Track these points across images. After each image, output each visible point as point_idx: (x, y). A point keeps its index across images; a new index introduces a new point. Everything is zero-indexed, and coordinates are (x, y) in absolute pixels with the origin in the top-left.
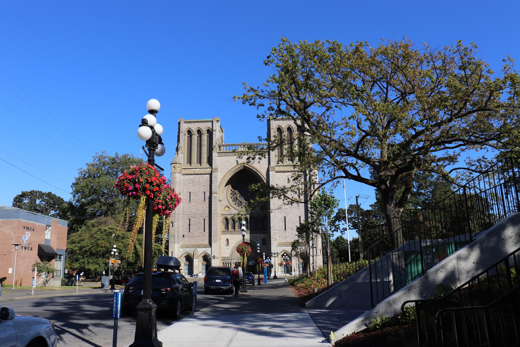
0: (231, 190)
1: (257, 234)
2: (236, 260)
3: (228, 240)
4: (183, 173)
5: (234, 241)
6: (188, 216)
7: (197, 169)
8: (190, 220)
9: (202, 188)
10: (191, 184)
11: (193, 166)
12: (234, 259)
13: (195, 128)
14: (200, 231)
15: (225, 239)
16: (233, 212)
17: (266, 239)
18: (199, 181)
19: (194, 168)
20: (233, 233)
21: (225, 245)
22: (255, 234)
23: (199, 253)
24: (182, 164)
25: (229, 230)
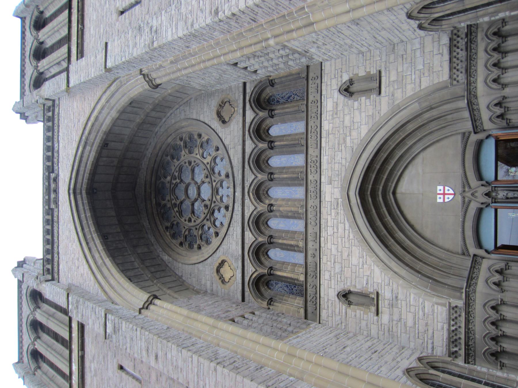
0: (181, 244)
2: (476, 260)
5: (354, 260)
9: (110, 373)
12: (471, 280)
15: (340, 307)
17: (346, 78)
20: (314, 256)
21: (372, 315)
22: (323, 140)
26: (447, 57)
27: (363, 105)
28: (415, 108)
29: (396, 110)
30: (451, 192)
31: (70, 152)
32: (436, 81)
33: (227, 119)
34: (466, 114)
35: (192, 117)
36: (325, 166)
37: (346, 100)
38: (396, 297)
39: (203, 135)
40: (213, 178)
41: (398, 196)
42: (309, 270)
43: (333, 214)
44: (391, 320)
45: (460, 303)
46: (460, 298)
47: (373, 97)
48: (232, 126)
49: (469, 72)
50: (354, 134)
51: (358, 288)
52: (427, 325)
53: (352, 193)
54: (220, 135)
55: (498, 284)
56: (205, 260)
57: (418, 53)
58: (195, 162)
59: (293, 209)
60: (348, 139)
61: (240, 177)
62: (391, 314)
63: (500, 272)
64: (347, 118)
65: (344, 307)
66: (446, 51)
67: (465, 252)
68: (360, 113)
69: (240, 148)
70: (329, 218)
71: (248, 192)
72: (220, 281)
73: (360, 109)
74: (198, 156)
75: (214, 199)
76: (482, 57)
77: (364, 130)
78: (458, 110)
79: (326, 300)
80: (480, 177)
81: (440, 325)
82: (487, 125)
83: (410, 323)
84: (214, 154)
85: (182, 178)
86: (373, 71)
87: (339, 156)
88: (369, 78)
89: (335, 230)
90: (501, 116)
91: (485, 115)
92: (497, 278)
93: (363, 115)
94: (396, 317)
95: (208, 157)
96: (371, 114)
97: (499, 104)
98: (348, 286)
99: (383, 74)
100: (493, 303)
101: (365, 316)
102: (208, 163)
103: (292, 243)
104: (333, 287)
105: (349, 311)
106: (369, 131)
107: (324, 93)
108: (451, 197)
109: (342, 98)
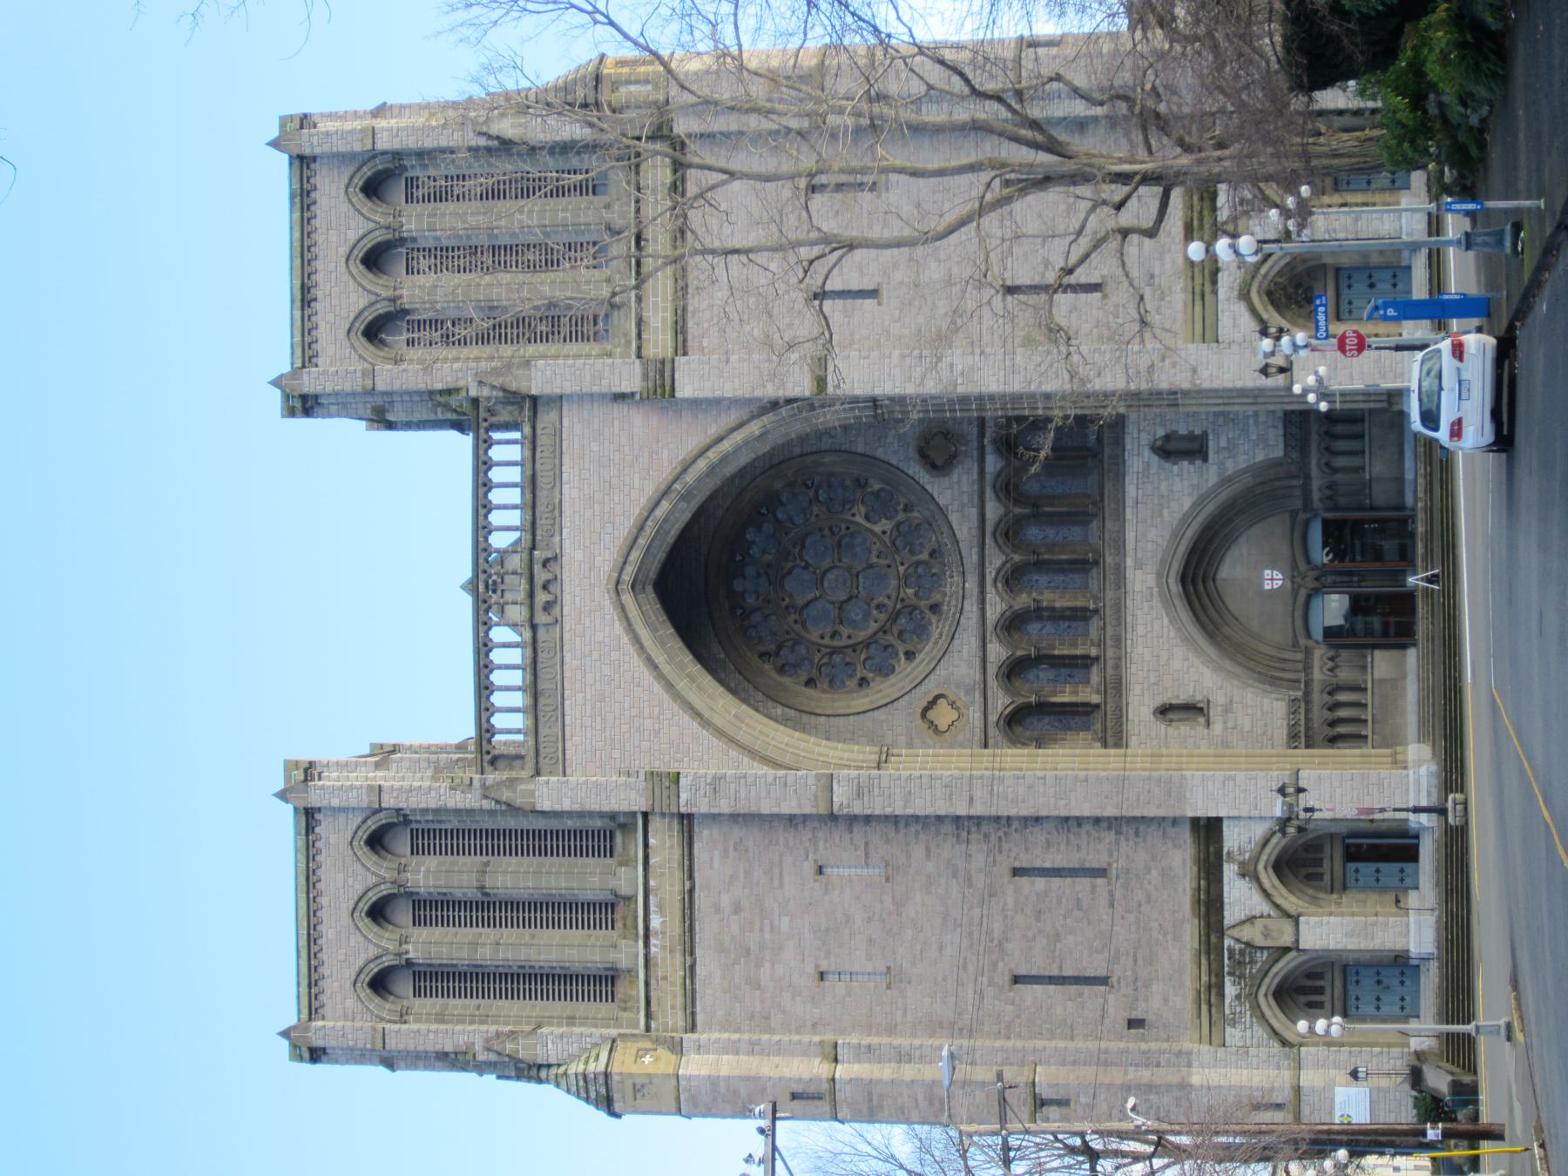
0: (810, 682)
1: (1129, 502)
2: (1308, 652)
3: (1164, 711)
4: (681, 1023)
5: (1177, 664)
6: (990, 992)
7: (655, 922)
8: (1017, 980)
10: (759, 965)
11: (627, 953)
12: (1307, 668)
13: (356, 939)
14: (1103, 901)
16: (964, 669)
17: (1161, 433)
18: (737, 909)
19: (647, 945)
20: (1117, 667)
21: (1200, 730)
22: (1129, 512)
23: (1258, 905)
24: (614, 1032)
25: (1096, 699)
26: (1281, 432)
27: (1185, 471)
28: (1247, 480)
29: (1226, 481)
30: (1280, 576)
31: (619, 510)
32: (1271, 456)
33: (939, 462)
34: (1298, 492)
35: (853, 449)
36: (1130, 545)
37: (1162, 462)
38: (1231, 701)
39: (871, 481)
40: (898, 560)
41: (1218, 582)
42: (1109, 686)
43: (1146, 609)
44: (1225, 729)
45: (1299, 694)
46: (1299, 689)
47: (1198, 463)
48: (955, 477)
49: (1304, 451)
50: (1174, 505)
51: (1182, 697)
52: (1266, 725)
53: (1172, 581)
54: (929, 488)
55: (1331, 670)
56: (892, 702)
57: (1251, 421)
58: (848, 528)
59: (1079, 604)
60: (1166, 512)
61: (975, 557)
62: (1225, 722)
63: (1332, 659)
64: (1164, 485)
65: (1163, 727)
66: (1280, 426)
67: (1295, 645)
68: (1182, 480)
69: (973, 512)
70: (1139, 613)
71: (995, 581)
72: (931, 731)
73: (1180, 475)
74: (858, 519)
75: (902, 595)
76: (1314, 437)
77: (1187, 503)
78: (1292, 487)
79: (1136, 722)
80: (1308, 561)
81: (1279, 722)
82: (1316, 504)
83: (1247, 727)
84: (901, 516)
85: (806, 558)
86: (1198, 432)
87: (1153, 533)
88: (1191, 437)
89: (1149, 629)
90: (1330, 498)
91: (1316, 495)
92: (1330, 664)
93: (1186, 483)
94: (1230, 725)
95: (884, 521)
96: (1195, 482)
97: (1329, 487)
98: (1169, 697)
99: (1211, 437)
100: (1328, 689)
101: (1193, 732)
102: (884, 532)
103: (1078, 652)
104: (1146, 703)
105: (1170, 730)
106: (1194, 504)
107: (1128, 447)
108: (1280, 582)
109: (1155, 459)
